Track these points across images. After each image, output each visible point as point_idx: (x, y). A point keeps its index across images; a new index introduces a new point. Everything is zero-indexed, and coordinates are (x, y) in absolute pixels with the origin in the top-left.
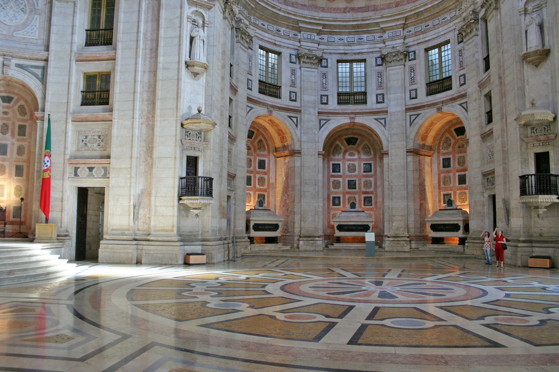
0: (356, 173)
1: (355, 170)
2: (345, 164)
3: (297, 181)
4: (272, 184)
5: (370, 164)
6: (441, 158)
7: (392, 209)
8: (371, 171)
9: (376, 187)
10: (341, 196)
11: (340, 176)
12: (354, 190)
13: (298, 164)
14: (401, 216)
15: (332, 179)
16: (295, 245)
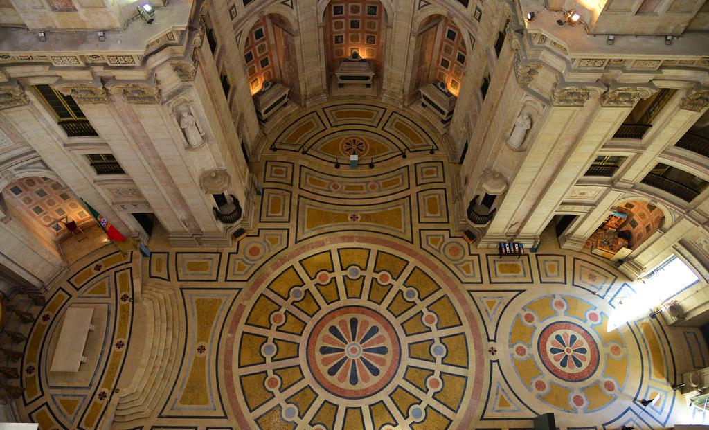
0: (359, 14)
1: (358, 11)
2: (348, 7)
3: (299, 57)
4: (273, 45)
5: (375, 8)
6: (448, 28)
7: (391, 74)
8: (375, 14)
9: (379, 29)
10: (344, 35)
11: (343, 18)
12: (357, 29)
13: (297, 42)
14: (399, 81)
15: (334, 21)
16: (303, 104)
